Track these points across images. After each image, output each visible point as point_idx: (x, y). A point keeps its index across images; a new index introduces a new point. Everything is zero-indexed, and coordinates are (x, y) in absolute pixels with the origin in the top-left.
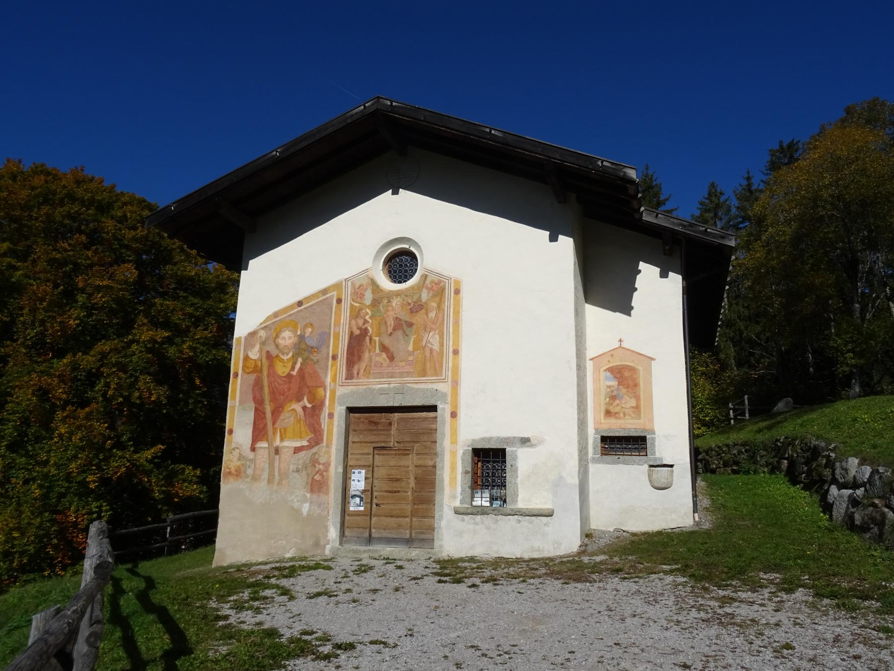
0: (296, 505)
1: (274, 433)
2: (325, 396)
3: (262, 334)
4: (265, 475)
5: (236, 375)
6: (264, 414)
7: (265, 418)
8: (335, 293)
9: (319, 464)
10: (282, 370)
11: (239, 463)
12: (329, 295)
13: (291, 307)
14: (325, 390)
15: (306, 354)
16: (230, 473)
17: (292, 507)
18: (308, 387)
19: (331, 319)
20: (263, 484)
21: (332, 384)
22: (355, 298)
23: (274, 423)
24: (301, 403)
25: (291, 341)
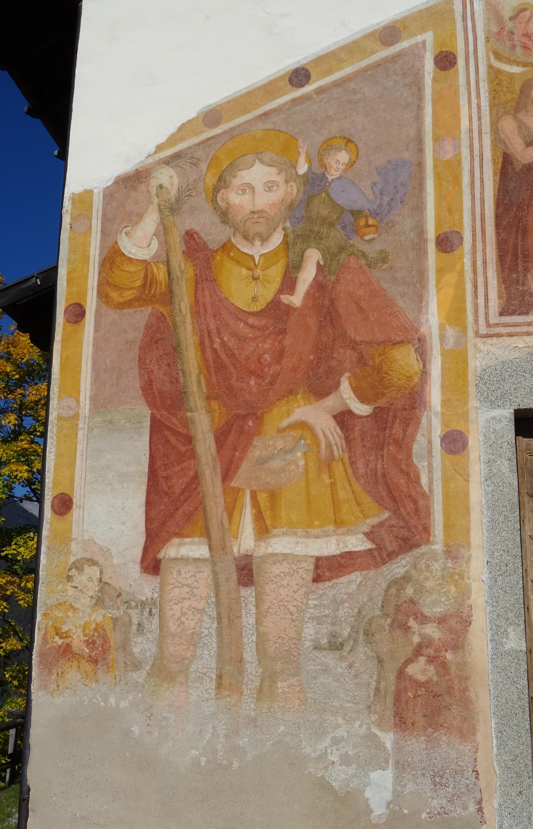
0: (339, 776)
1: (232, 509)
2: (425, 373)
3: (168, 178)
4: (206, 660)
5: (77, 313)
6: (189, 440)
7: (192, 454)
8: (428, 36)
9: (423, 619)
10: (245, 291)
11: (98, 617)
12: (404, 44)
13: (269, 89)
14: (423, 354)
15: (336, 235)
16: (66, 651)
17: (324, 785)
18: (354, 345)
19: (419, 118)
20: (199, 693)
21: (451, 333)
22: (505, 52)
23: (227, 474)
24: (330, 402)
25: (276, 196)
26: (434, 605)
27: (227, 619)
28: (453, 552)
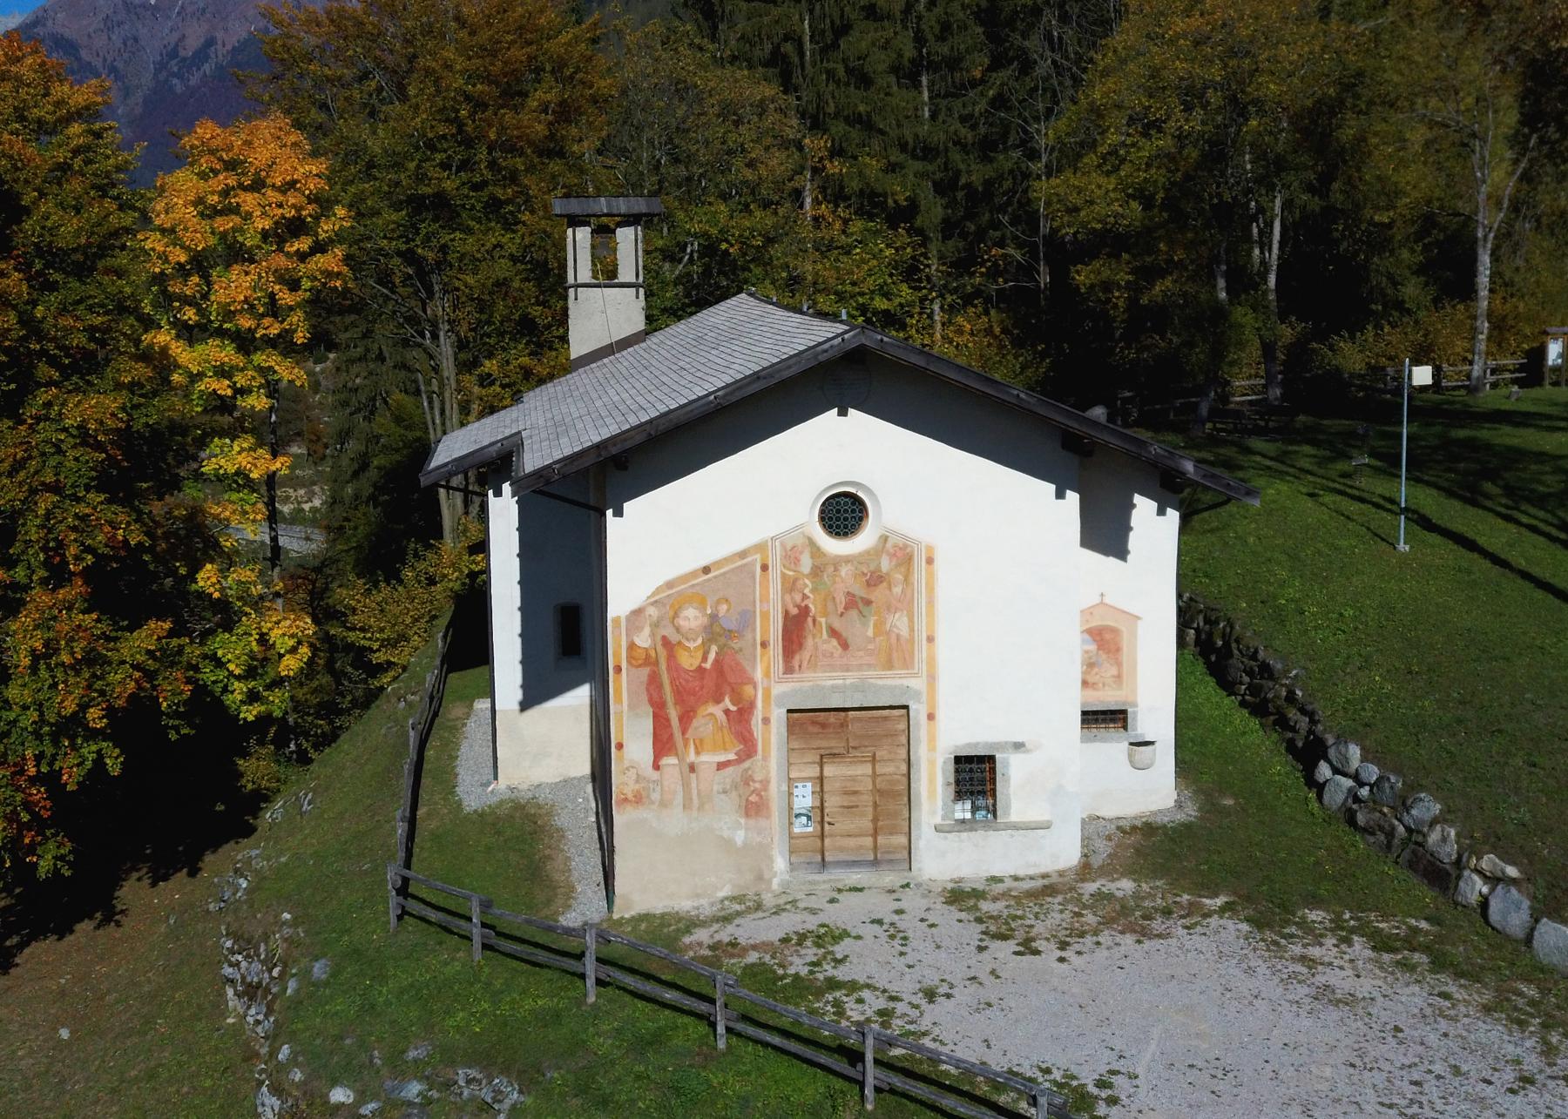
0: (726, 834)
4: (679, 799)
7: (670, 726)
8: (758, 556)
10: (688, 661)
11: (637, 787)
13: (694, 574)
16: (626, 800)
24: (722, 706)
25: (699, 622)
26: (758, 777)
27: (686, 785)
28: (765, 758)
